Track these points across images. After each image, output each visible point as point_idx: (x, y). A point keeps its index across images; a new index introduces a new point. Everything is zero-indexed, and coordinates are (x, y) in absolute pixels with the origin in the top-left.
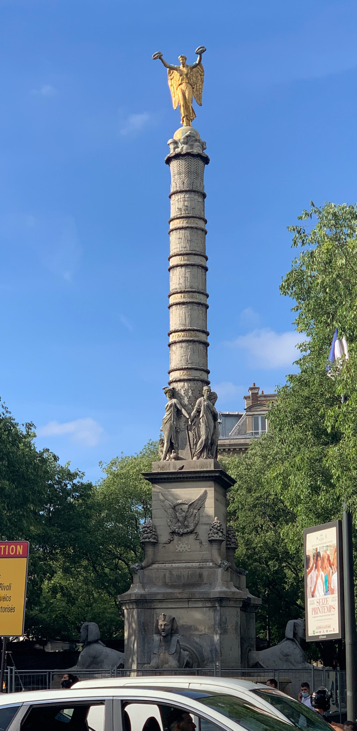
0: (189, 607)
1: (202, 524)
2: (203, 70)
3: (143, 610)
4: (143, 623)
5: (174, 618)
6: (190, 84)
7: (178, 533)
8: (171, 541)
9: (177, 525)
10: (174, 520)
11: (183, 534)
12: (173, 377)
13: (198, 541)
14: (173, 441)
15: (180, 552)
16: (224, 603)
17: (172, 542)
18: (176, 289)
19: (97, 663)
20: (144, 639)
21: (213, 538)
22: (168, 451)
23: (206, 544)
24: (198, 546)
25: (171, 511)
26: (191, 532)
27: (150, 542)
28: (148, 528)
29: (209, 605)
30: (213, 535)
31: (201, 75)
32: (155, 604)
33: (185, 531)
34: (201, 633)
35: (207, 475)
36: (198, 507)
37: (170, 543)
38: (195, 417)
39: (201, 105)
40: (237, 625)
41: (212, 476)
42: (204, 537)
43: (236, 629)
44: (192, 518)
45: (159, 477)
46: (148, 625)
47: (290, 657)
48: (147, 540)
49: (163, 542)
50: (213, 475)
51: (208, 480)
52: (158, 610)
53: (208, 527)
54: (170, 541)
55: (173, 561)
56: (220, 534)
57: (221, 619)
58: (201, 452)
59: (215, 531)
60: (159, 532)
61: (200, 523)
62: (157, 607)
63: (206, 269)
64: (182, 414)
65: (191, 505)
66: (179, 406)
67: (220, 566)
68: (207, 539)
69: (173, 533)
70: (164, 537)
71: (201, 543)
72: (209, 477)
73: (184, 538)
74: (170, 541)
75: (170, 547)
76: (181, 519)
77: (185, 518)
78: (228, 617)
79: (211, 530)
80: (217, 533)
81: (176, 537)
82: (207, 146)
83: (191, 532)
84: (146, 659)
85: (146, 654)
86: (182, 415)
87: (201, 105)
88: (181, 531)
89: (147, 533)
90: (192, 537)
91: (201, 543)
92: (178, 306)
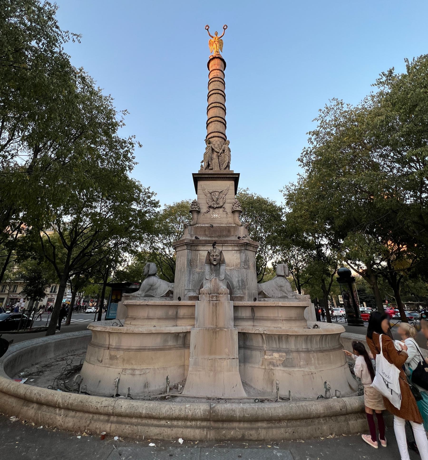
3: (191, 251)
4: (190, 260)
7: (213, 207)
9: (212, 203)
10: (211, 200)
11: (217, 208)
15: (214, 218)
16: (248, 248)
19: (153, 290)
20: (190, 271)
23: (230, 214)
24: (225, 215)
25: (209, 195)
27: (196, 210)
29: (236, 248)
32: (199, 247)
33: (218, 206)
34: (231, 268)
35: (231, 176)
36: (225, 193)
43: (254, 267)
44: (221, 199)
45: (203, 176)
46: (193, 262)
48: (194, 209)
50: (235, 176)
52: (201, 252)
53: (231, 205)
54: (208, 212)
56: (240, 207)
57: (246, 258)
60: (201, 207)
61: (226, 202)
65: (221, 192)
66: (213, 147)
67: (241, 226)
68: (231, 211)
69: (210, 207)
70: (204, 209)
71: (227, 213)
73: (216, 210)
74: (208, 212)
75: (208, 215)
76: (215, 199)
77: (217, 199)
81: (211, 210)
83: (221, 207)
84: (191, 286)
85: (191, 282)
88: (215, 206)
90: (221, 210)
91: (227, 213)
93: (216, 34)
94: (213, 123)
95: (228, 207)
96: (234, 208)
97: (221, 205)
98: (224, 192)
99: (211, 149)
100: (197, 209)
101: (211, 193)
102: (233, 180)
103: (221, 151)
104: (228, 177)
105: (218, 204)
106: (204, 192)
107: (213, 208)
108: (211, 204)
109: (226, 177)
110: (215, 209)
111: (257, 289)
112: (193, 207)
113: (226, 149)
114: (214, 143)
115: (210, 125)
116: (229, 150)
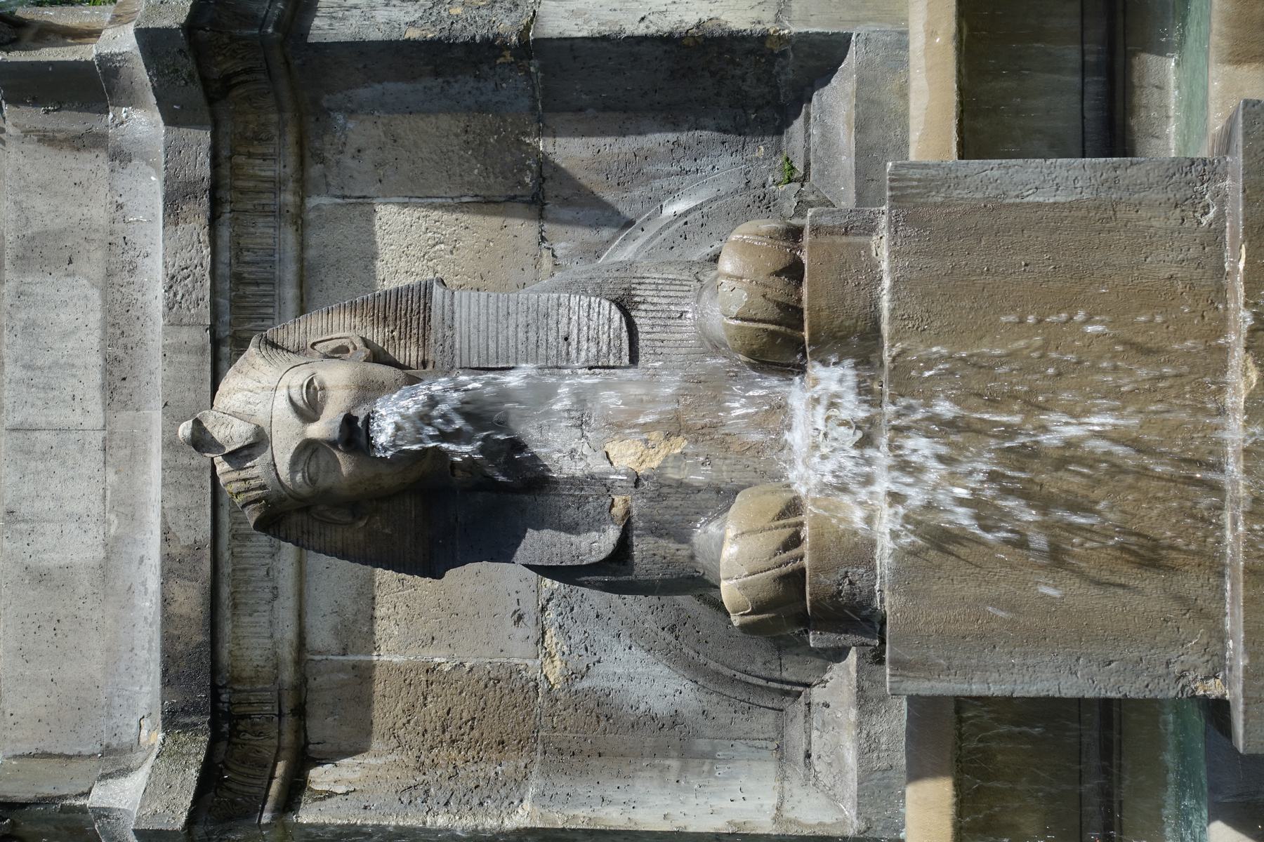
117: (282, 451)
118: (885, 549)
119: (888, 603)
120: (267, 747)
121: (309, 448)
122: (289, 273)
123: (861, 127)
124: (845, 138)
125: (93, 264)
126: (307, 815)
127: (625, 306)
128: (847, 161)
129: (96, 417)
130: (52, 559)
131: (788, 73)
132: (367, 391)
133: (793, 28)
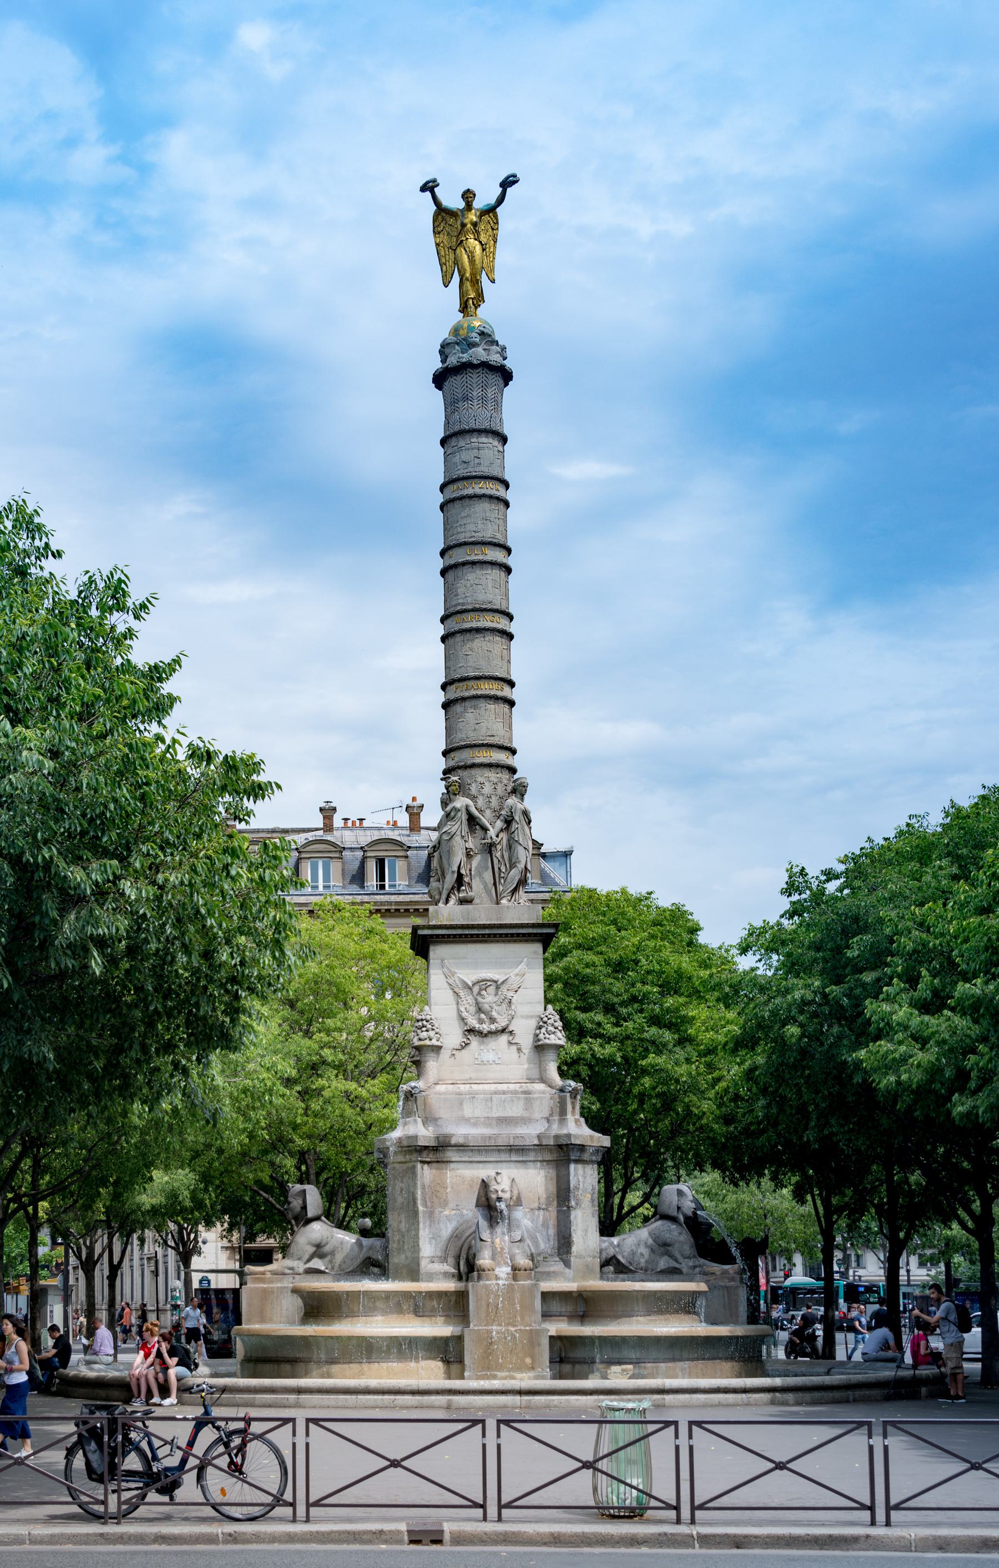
0: (511, 1161)
1: (522, 1017)
2: (497, 219)
5: (483, 1181)
6: (480, 242)
8: (467, 1044)
11: (490, 1033)
12: (456, 759)
13: (514, 1047)
14: (463, 872)
17: (468, 1048)
18: (463, 604)
21: (547, 1041)
22: (453, 888)
26: (503, 1031)
28: (427, 1021)
30: (547, 1036)
31: (493, 229)
33: (493, 1027)
37: (463, 1048)
38: (502, 830)
39: (493, 281)
40: (594, 1193)
41: (541, 934)
42: (526, 1041)
47: (670, 1248)
48: (427, 1042)
49: (452, 1046)
51: (533, 941)
53: (533, 1023)
54: (465, 1046)
55: (470, 1079)
56: (559, 1034)
58: (515, 890)
59: (551, 1028)
62: (453, 1159)
63: (508, 570)
64: (478, 824)
65: (503, 982)
69: (471, 1031)
71: (519, 1050)
72: (535, 935)
78: (581, 1179)
79: (540, 1028)
80: (554, 1033)
81: (475, 1041)
82: (509, 353)
83: (503, 1031)
86: (477, 827)
87: (493, 281)
88: (485, 1027)
89: (427, 1031)
90: (504, 1038)
92: (468, 635)
93: (468, 196)
94: (467, 704)
95: (524, 1030)
96: (541, 1036)
97: (504, 1024)
98: (510, 982)
99: (464, 817)
100: (434, 1042)
101: (470, 989)
102: (538, 941)
103: (499, 824)
104: (524, 935)
105: (493, 1020)
106: (451, 981)
107: (480, 1034)
108: (473, 1022)
109: (518, 935)
110: (486, 1035)
111: (598, 1255)
112: (424, 1035)
113: (517, 818)
114: (474, 789)
115: (458, 708)
116: (525, 813)
117: (497, 1187)
118: (488, 1282)
119: (481, 1283)
120: (431, 1156)
121: (497, 1191)
122: (524, 1159)
123: (553, 1272)
124: (552, 1269)
125: (526, 1114)
126: (419, 1165)
127: (520, 1241)
128: (547, 1269)
129: (494, 1115)
130: (465, 1106)
131: (564, 1257)
132: (506, 1201)
133: (572, 1259)
